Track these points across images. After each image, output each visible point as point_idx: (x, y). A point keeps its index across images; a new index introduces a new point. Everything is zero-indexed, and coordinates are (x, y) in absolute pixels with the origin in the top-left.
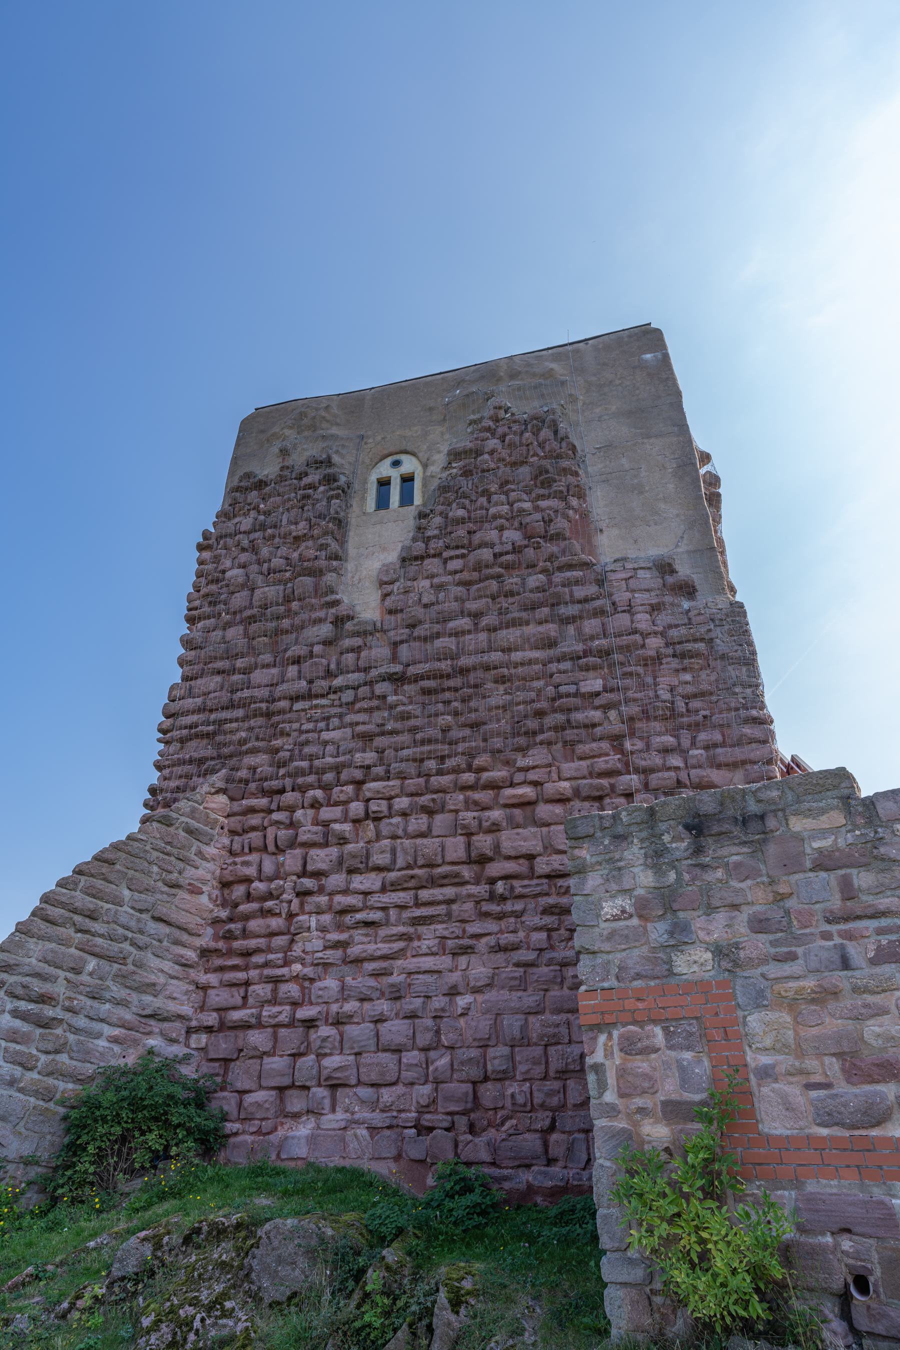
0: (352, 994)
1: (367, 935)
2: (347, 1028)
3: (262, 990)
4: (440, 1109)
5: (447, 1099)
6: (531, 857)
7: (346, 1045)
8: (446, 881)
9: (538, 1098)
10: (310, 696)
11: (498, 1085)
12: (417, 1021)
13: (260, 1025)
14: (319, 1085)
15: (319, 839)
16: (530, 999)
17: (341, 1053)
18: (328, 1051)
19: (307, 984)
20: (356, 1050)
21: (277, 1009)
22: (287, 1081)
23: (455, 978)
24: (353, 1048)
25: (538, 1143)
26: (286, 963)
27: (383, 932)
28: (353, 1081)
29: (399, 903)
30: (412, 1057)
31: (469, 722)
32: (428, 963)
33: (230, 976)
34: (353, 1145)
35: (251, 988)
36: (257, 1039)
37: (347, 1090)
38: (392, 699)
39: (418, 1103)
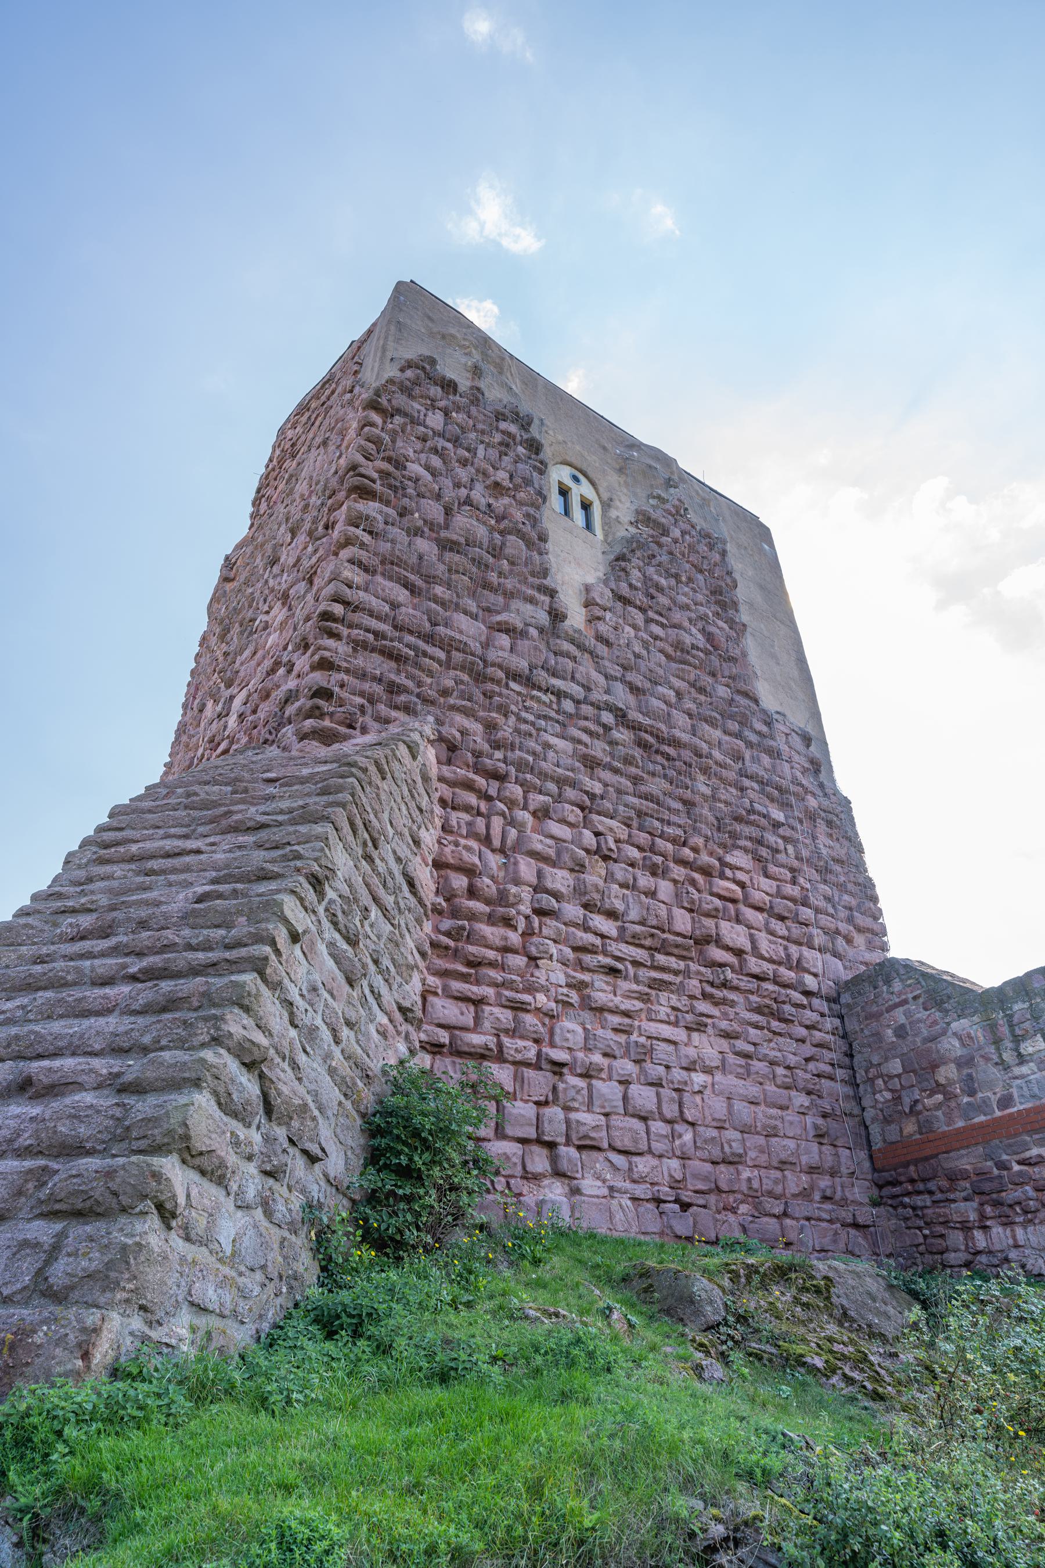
0: (599, 1045)
1: (607, 983)
2: (594, 1082)
3: (505, 1016)
4: (690, 1187)
5: (695, 1176)
6: (739, 953)
7: (597, 1103)
8: (676, 951)
9: (768, 1185)
10: (529, 682)
11: (731, 1168)
12: (661, 1090)
13: (500, 1057)
14: (568, 1143)
15: (552, 852)
16: (753, 1090)
17: (588, 1111)
18: (576, 1105)
19: (547, 1021)
20: (607, 1110)
21: (521, 1043)
22: (533, 1135)
23: (691, 1052)
24: (603, 1107)
25: (778, 1226)
26: (531, 989)
27: (624, 985)
28: (606, 1145)
29: (638, 959)
30: (658, 1127)
31: (685, 797)
32: (667, 1031)
33: (456, 986)
34: (619, 1216)
35: (487, 1009)
36: (502, 1074)
37: (595, 1154)
38: (616, 735)
39: (671, 1176)
